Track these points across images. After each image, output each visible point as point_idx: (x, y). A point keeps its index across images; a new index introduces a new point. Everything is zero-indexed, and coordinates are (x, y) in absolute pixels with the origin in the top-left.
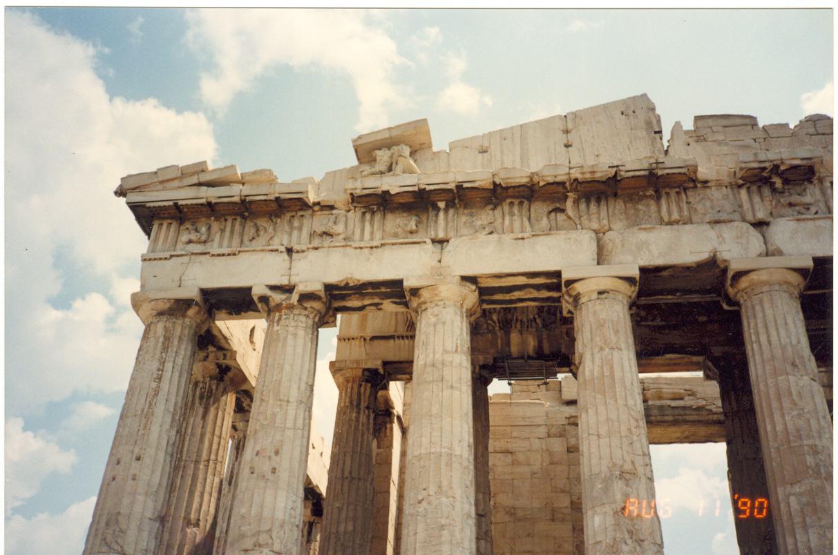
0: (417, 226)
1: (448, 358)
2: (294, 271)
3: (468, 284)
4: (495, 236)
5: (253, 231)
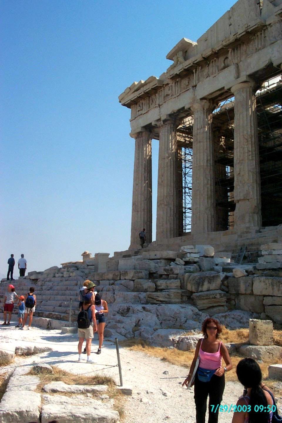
0: (188, 82)
3: (203, 100)
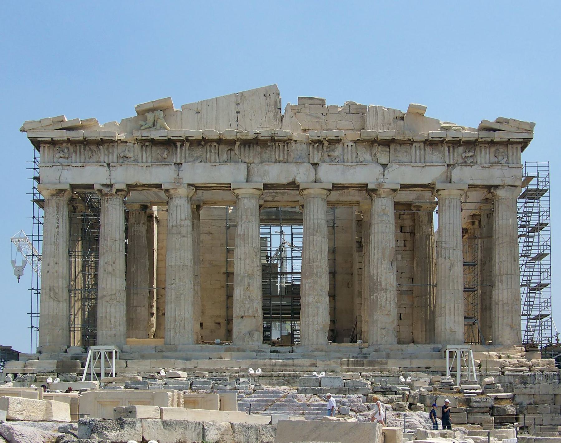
1: (182, 223)
2: (112, 177)
4: (203, 164)
5: (90, 153)
